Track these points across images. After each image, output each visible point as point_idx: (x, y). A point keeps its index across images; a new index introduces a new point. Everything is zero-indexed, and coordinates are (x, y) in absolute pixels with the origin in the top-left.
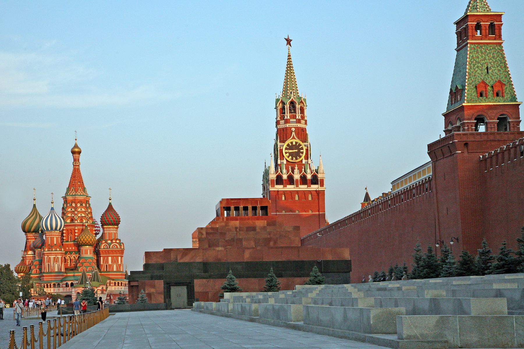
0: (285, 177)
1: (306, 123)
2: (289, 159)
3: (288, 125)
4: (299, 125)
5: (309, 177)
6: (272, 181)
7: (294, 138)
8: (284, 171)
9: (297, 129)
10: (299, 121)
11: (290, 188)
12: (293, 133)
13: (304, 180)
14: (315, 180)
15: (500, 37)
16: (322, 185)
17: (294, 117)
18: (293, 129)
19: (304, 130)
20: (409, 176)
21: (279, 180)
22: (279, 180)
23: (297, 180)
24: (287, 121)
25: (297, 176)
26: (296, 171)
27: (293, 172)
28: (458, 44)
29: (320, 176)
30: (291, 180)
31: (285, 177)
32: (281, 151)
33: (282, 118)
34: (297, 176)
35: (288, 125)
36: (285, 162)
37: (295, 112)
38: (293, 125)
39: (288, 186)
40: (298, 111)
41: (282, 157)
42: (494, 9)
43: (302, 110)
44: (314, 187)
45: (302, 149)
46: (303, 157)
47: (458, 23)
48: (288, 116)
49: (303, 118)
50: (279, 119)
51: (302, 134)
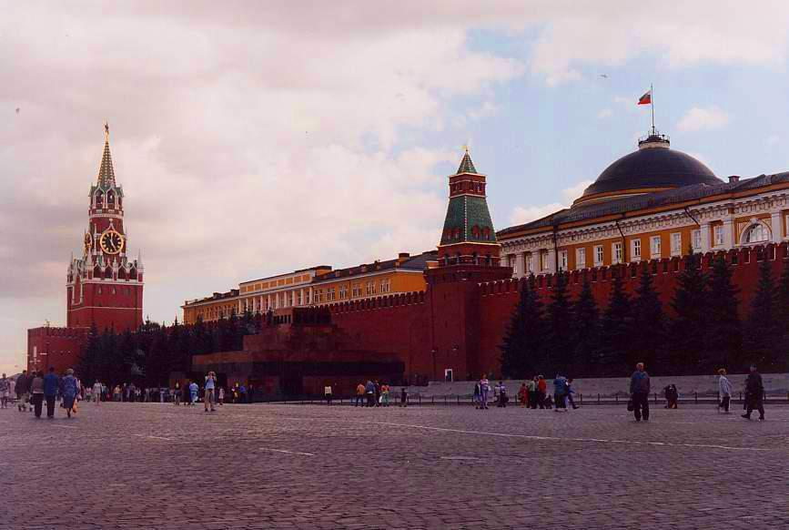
0: (103, 269)
1: (122, 215)
2: (106, 251)
3: (105, 215)
4: (117, 216)
5: (128, 271)
6: (90, 272)
7: (111, 229)
8: (103, 263)
9: (115, 219)
10: (117, 212)
11: (108, 281)
12: (111, 224)
13: (122, 274)
14: (133, 274)
15: (484, 193)
16: (141, 280)
17: (112, 207)
18: (111, 220)
19: (120, 221)
20: (290, 285)
21: (97, 273)
22: (97, 273)
23: (115, 274)
24: (105, 211)
25: (115, 269)
26: (115, 263)
27: (112, 265)
28: (452, 194)
29: (139, 271)
30: (108, 274)
31: (103, 269)
32: (98, 241)
33: (99, 207)
34: (115, 269)
35: (105, 215)
36: (101, 253)
37: (114, 202)
38: (110, 216)
39: (107, 280)
40: (117, 201)
41: (99, 248)
42: (480, 172)
43: (120, 202)
44: (133, 282)
45: (120, 241)
46: (120, 250)
47: (452, 179)
48: (105, 205)
49: (121, 208)
50: (95, 208)
51: (118, 225)
